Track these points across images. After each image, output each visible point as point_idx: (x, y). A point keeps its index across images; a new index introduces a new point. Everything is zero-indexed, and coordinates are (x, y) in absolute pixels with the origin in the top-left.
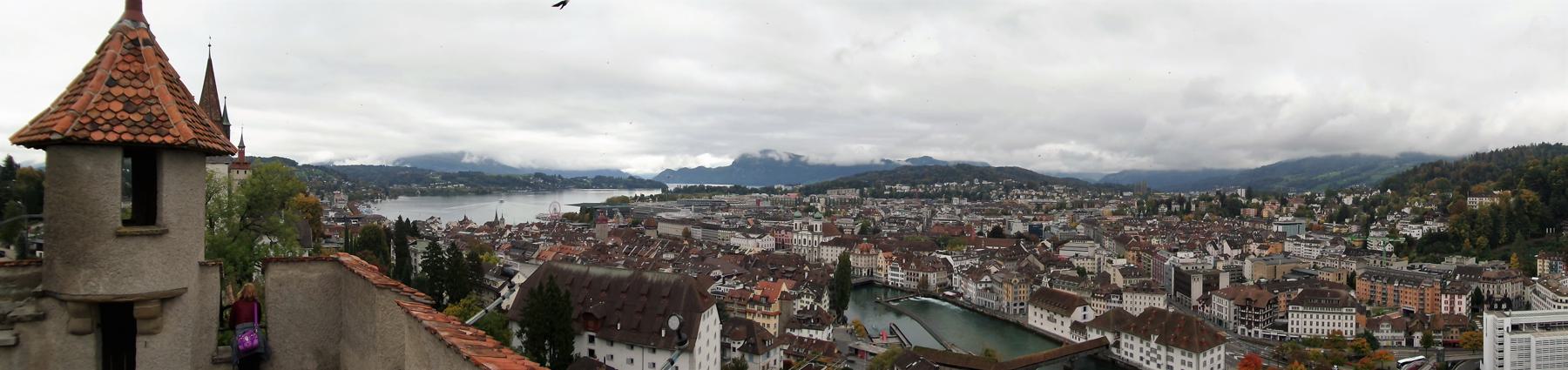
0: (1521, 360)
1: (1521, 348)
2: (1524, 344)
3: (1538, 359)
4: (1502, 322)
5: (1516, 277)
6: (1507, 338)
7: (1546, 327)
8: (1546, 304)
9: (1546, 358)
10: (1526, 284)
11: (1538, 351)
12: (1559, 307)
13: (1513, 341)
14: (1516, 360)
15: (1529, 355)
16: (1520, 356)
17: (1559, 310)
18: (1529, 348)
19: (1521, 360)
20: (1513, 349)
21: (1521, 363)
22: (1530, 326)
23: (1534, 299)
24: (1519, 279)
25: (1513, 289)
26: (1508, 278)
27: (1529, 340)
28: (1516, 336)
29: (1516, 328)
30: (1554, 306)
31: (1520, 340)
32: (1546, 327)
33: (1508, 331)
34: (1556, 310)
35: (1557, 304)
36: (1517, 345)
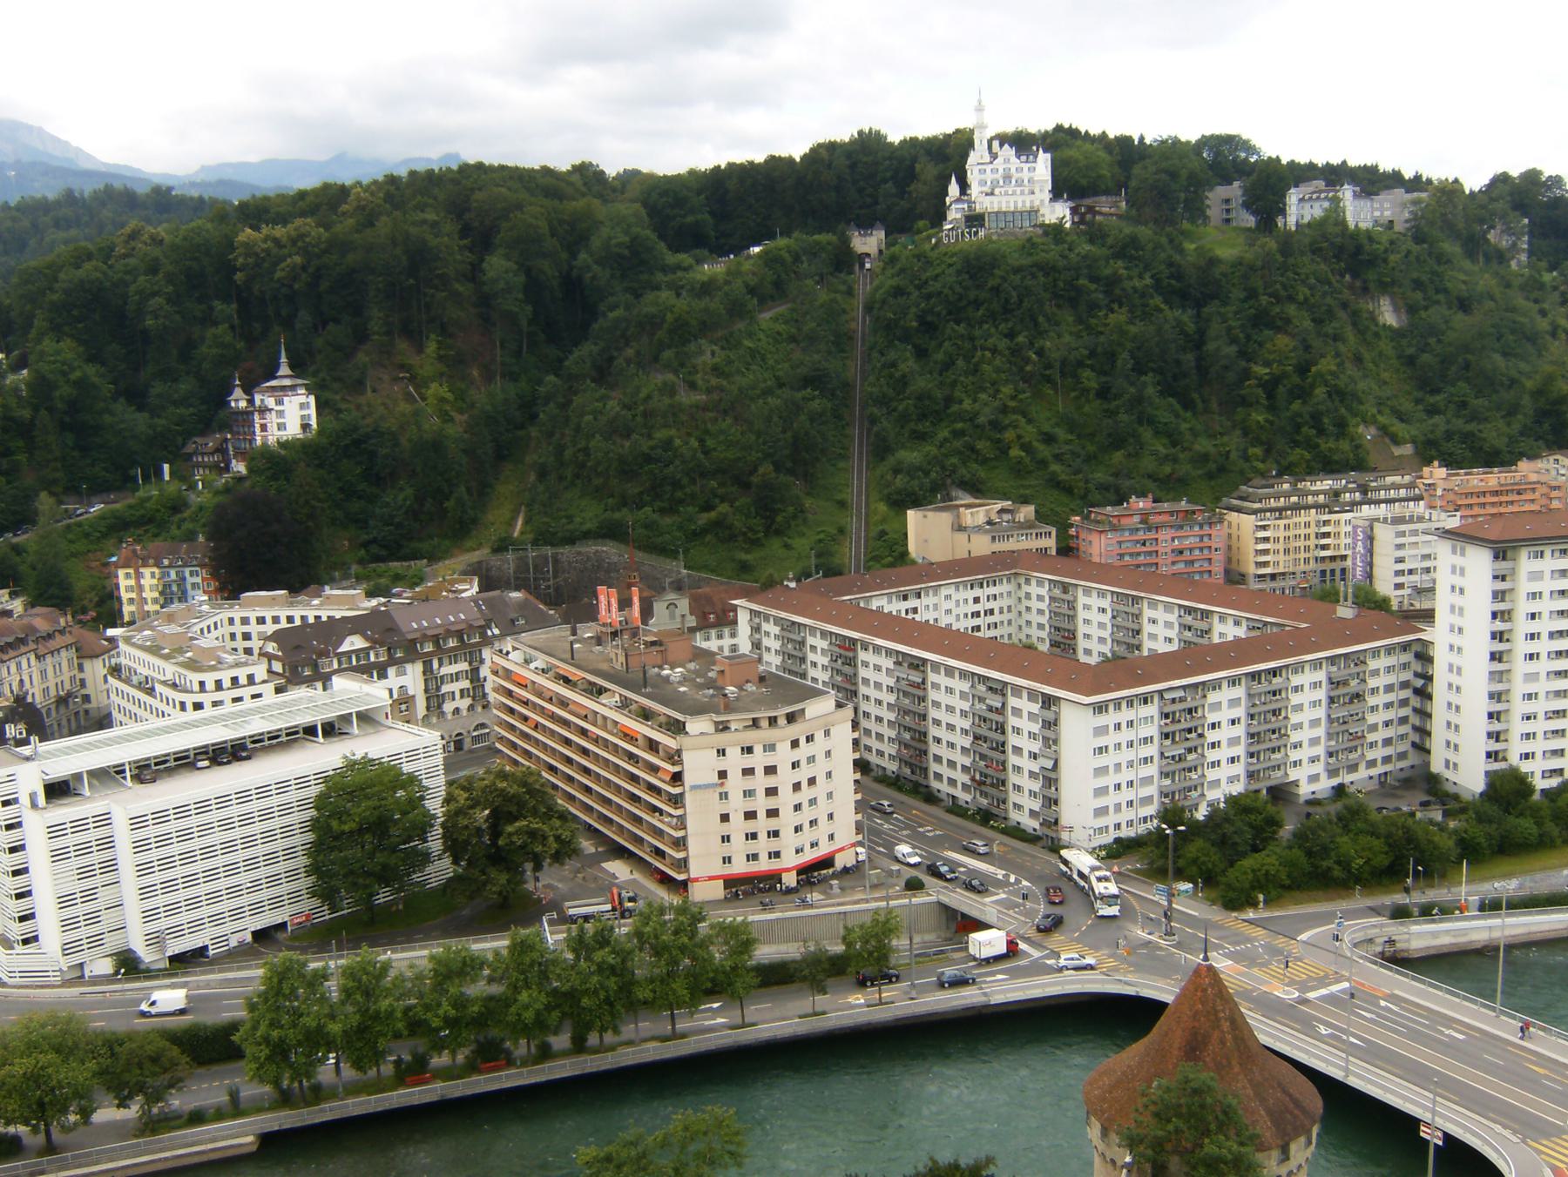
0: (88, 883)
1: (84, 849)
2: (93, 835)
3: (143, 869)
4: (11, 779)
5: (50, 636)
6: (36, 826)
7: (147, 772)
8: (155, 703)
9: (166, 863)
10: (85, 654)
11: (140, 846)
12: (198, 706)
13: (55, 831)
14: (77, 887)
15: (111, 866)
16: (85, 873)
17: (199, 714)
18: (108, 843)
19: (88, 883)
20: (58, 856)
21: (89, 895)
22: (107, 776)
23: (117, 696)
24: (59, 641)
25: (44, 673)
26: (22, 641)
27: (104, 820)
28: (66, 812)
29: (58, 790)
30: (183, 706)
31: (79, 825)
32: (147, 772)
33: (34, 805)
34: (191, 715)
35: (190, 699)
36: (71, 840)
